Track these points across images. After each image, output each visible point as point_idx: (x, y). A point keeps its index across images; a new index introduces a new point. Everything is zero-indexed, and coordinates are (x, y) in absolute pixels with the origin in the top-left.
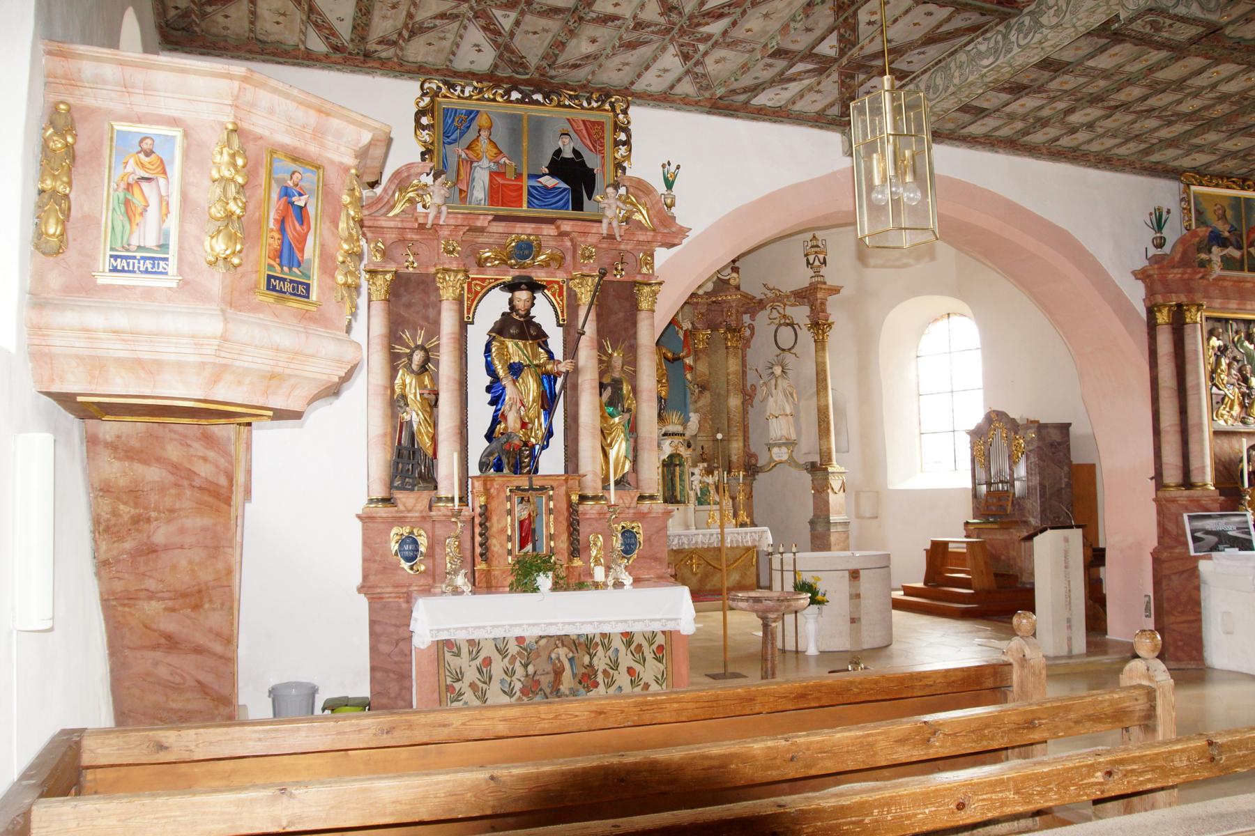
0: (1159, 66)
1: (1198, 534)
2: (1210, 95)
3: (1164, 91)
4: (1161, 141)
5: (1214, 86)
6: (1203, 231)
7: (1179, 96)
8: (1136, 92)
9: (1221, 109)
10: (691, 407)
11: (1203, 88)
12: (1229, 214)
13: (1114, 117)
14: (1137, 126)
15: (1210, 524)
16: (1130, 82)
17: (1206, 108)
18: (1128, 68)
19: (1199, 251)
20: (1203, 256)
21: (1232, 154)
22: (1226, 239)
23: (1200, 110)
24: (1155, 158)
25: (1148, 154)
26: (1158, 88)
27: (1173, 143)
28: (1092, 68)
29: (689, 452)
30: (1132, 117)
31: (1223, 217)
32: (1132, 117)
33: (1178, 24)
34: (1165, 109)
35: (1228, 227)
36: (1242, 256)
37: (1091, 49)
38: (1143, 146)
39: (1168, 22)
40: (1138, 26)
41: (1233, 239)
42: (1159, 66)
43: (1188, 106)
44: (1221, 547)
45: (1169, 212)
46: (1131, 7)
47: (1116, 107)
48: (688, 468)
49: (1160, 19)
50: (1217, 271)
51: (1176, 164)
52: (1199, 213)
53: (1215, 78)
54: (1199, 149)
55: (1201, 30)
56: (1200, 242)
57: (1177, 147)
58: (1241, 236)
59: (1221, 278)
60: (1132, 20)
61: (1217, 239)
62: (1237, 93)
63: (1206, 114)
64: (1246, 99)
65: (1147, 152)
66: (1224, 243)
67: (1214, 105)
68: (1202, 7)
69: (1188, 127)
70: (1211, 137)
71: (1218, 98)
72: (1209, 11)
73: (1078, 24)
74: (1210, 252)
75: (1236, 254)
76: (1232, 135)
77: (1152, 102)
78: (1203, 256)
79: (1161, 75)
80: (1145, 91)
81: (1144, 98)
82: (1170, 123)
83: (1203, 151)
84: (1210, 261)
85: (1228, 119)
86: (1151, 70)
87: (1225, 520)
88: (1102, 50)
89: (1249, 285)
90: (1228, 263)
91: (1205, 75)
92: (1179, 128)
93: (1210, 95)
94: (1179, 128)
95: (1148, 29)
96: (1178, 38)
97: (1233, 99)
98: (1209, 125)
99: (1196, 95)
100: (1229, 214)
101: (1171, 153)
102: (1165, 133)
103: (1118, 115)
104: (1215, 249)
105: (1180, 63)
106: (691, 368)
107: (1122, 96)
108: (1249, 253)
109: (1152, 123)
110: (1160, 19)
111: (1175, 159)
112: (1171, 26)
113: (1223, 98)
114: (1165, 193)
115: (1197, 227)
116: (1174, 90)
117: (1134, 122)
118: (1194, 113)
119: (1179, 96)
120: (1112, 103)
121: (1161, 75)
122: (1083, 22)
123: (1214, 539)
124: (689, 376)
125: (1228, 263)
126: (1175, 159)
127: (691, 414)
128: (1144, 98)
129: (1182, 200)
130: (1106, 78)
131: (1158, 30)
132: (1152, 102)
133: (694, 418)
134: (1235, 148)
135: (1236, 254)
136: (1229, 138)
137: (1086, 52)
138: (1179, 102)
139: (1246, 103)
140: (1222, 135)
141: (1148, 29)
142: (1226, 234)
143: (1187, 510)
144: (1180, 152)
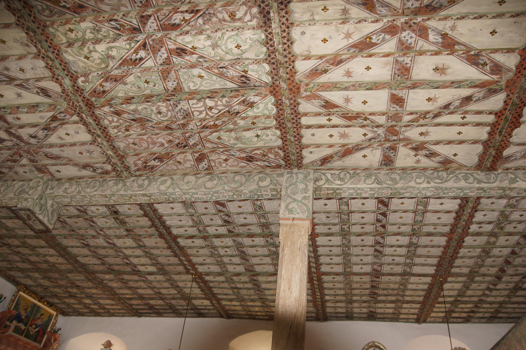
0: (29, 237)
2: (42, 258)
3: (27, 248)
4: (17, 267)
5: (45, 256)
6: (14, 312)
7: (31, 253)
8: (16, 242)
9: (44, 266)
11: (41, 254)
12: (29, 309)
13: (2, 248)
14: (11, 256)
16: (15, 237)
17: (39, 263)
18: (17, 231)
19: (8, 320)
20: (8, 323)
21: (41, 286)
22: (22, 319)
23: (37, 262)
24: (12, 273)
25: (9, 270)
26: (25, 245)
27: (22, 270)
28: (3, 223)
30: (10, 252)
31: (26, 310)
32: (10, 252)
33: (37, 221)
34: (24, 255)
35: (25, 315)
36: (25, 329)
37: (6, 215)
38: (9, 266)
39: (34, 219)
40: (22, 213)
41: (25, 321)
42: (29, 237)
43: (33, 258)
45: (5, 298)
46: (24, 205)
47: (6, 244)
49: (31, 215)
50: (10, 332)
51: (19, 280)
52: (18, 304)
53: (47, 253)
54: (30, 277)
55: (44, 229)
56: (11, 317)
57: (22, 273)
59: (10, 336)
60: (21, 209)
61: (18, 318)
62: (52, 263)
63: (38, 265)
64: (54, 267)
65: (10, 269)
66: (20, 320)
67: (42, 263)
68: (48, 220)
69: (30, 267)
70: (37, 275)
71: (45, 261)
72: (50, 223)
73: (4, 201)
74: (12, 322)
75: (23, 327)
76: (44, 278)
77: (21, 250)
78: (8, 323)
79: (29, 241)
80: (20, 244)
81: (18, 247)
82: (23, 262)
83: (31, 279)
84: (10, 326)
85: (46, 271)
86: (25, 237)
88: (11, 218)
89: (21, 343)
90: (17, 330)
91: (43, 249)
92: (26, 266)
93: (42, 258)
94: (26, 266)
95: (25, 217)
96: (35, 226)
97: (50, 264)
98: (37, 270)
99: (38, 256)
100: (29, 309)
101: (19, 274)
102: (20, 265)
103: (4, 248)
104: (14, 322)
105: (37, 240)
107: (10, 241)
108: (28, 329)
109: (17, 258)
110: (31, 215)
111: (20, 277)
112: (34, 220)
113: (46, 262)
115: (13, 309)
116: (31, 249)
117: (10, 254)
118: (34, 262)
119: (31, 253)
120: (5, 242)
121: (29, 241)
122: (6, 201)
125: (17, 330)
126: (20, 277)
128: (18, 247)
129: (14, 295)
130: (7, 230)
131: (30, 219)
132: (21, 250)
134: (43, 284)
135: (23, 327)
136: (43, 279)
137: (4, 215)
138: (30, 255)
139: (54, 268)
140: (41, 277)
141: (25, 217)
142: (23, 317)
144: (23, 276)
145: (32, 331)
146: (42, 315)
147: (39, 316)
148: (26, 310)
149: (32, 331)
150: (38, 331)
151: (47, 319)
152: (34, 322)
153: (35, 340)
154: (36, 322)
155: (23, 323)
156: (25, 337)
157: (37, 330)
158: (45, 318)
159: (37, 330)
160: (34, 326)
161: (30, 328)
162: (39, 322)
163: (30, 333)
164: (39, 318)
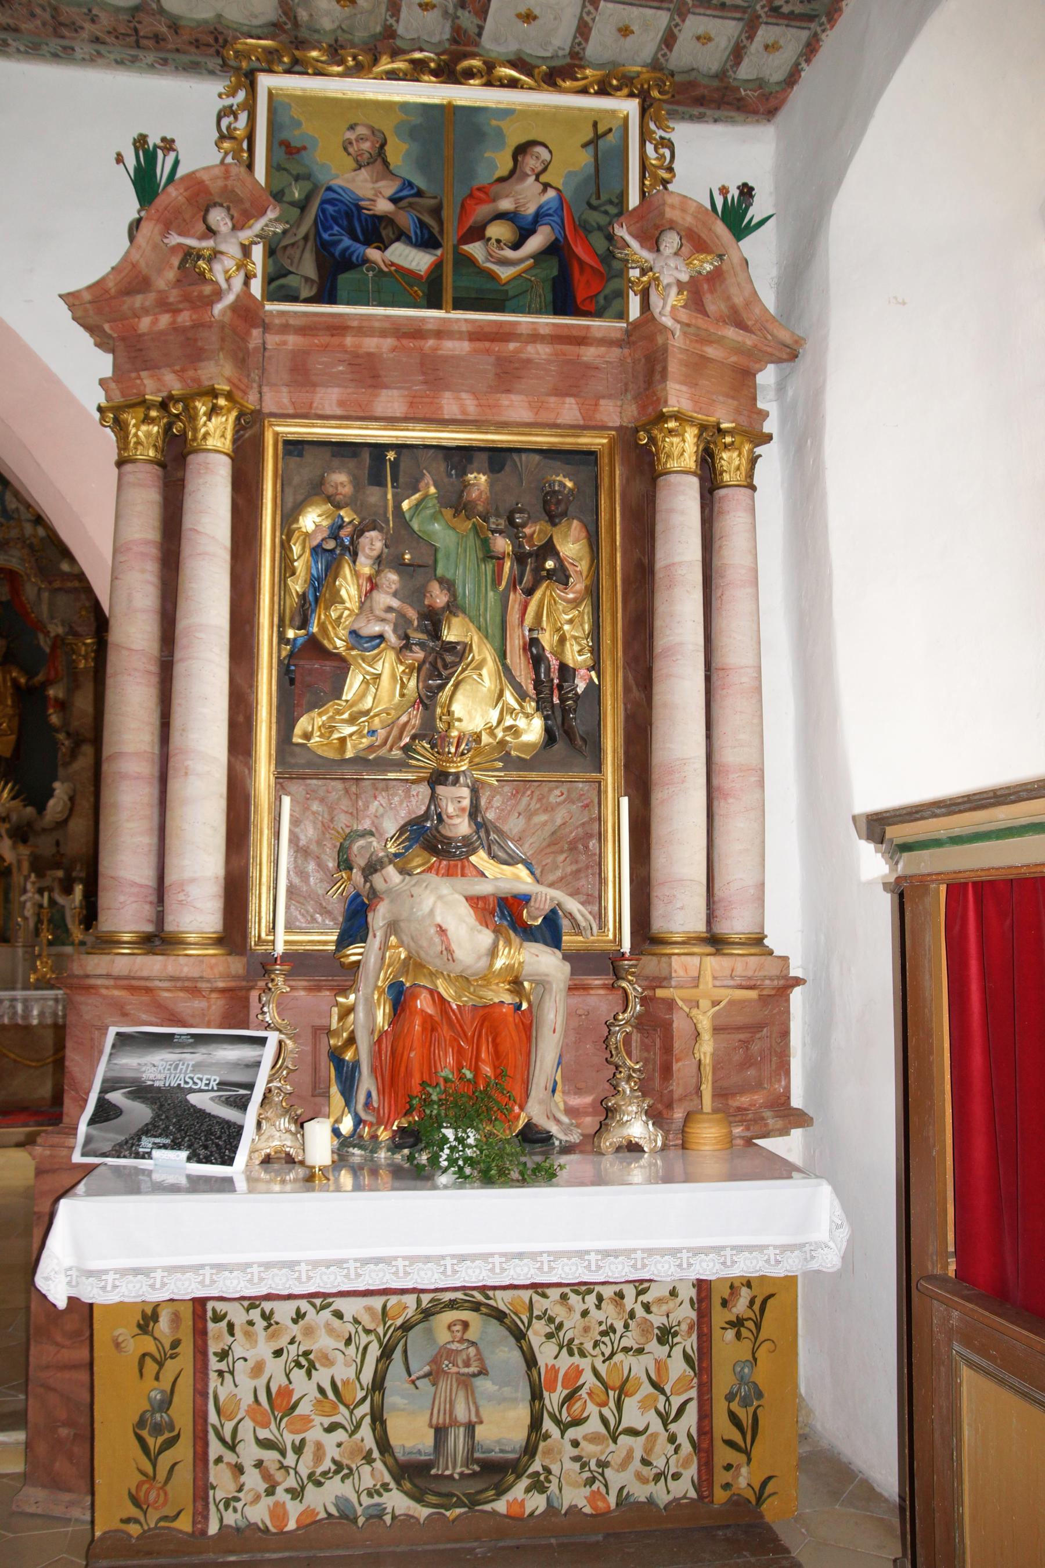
1: (116, 1097)
10: (61, 772)
12: (399, 153)
15: (157, 1067)
29: (24, 851)
31: (378, 158)
35: (390, 188)
36: (437, 267)
41: (406, 220)
44: (146, 1142)
48: (17, 879)
52: (287, 151)
58: (436, 212)
87: (200, 1054)
100: (398, 152)
106: (63, 706)
108: (465, 261)
114: (185, 111)
123: (140, 1112)
124: (55, 719)
127: (57, 785)
133: (60, 789)
142: (384, 206)
143: (124, 1015)
145: (504, 262)
146: (522, 150)
147: (504, 163)
148: (379, 156)
149: (504, 262)
150: (553, 250)
151: (585, 158)
152: (483, 210)
153: (563, 302)
154: (506, 205)
155: (400, 235)
156: (459, 304)
157: (535, 243)
158: (569, 162)
159: (535, 243)
160: (497, 231)
161: (476, 250)
162: (529, 197)
163: (492, 276)
164: (514, 173)
